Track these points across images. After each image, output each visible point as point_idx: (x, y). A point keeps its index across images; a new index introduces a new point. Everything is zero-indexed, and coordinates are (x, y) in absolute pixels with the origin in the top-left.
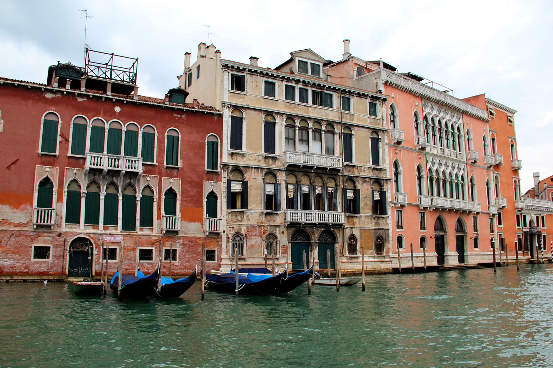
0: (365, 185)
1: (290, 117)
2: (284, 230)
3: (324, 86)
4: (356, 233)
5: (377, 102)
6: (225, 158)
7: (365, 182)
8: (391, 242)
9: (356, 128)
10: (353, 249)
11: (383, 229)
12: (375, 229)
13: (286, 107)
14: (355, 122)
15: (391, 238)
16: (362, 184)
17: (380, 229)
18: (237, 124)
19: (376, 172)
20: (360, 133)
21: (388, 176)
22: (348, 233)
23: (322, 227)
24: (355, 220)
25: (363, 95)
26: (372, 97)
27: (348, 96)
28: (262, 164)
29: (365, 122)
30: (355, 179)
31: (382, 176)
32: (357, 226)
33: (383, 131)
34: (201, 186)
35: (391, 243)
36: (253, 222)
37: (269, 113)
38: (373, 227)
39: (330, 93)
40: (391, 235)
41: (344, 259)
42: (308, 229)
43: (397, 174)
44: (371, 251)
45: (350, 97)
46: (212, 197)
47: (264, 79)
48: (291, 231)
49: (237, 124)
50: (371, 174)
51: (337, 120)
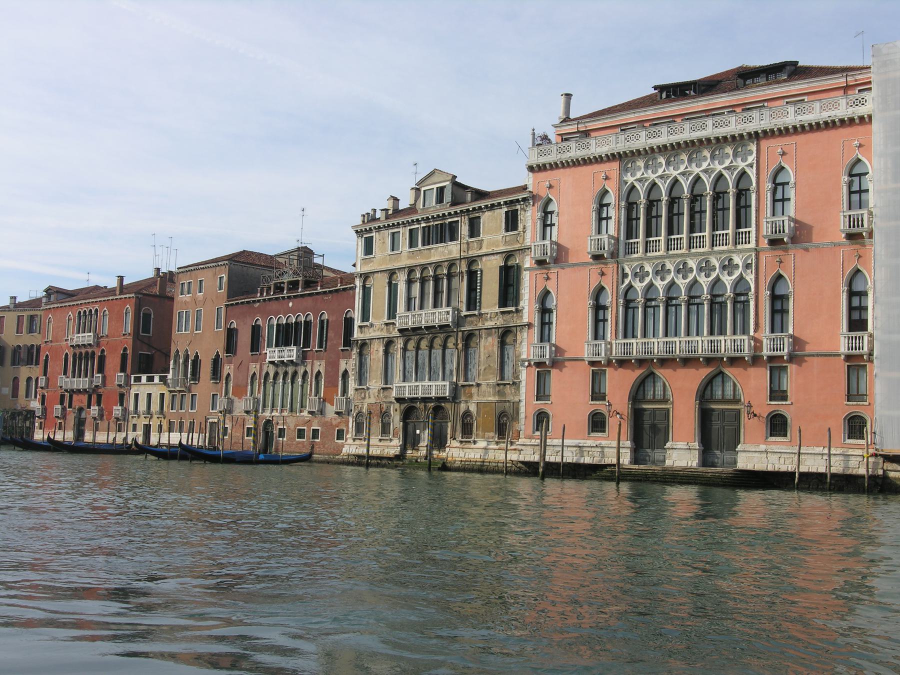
0: (490, 339)
1: (411, 270)
2: (397, 405)
3: (444, 214)
4: (473, 408)
5: (518, 207)
6: (357, 335)
7: (489, 335)
8: (522, 421)
9: (484, 259)
10: (467, 430)
11: (509, 401)
12: (498, 402)
13: (409, 258)
14: (484, 250)
15: (522, 416)
16: (486, 338)
17: (505, 402)
18: (366, 291)
19: (508, 317)
20: (488, 263)
21: (525, 320)
22: (463, 407)
23: (431, 402)
24: (474, 390)
25: (493, 205)
26: (506, 203)
27: (477, 215)
28: (385, 334)
29: (498, 246)
30: (477, 332)
31: (513, 321)
32: (476, 399)
33: (522, 250)
34: (337, 366)
35: (525, 422)
36: (372, 400)
37: (392, 273)
38: (497, 398)
39: (455, 219)
40: (522, 409)
41: (455, 443)
42: (418, 405)
43: (545, 311)
44: (492, 434)
45: (480, 214)
46: (345, 374)
47: (391, 231)
48: (403, 406)
49: (366, 291)
50: (499, 322)
51: (458, 256)
